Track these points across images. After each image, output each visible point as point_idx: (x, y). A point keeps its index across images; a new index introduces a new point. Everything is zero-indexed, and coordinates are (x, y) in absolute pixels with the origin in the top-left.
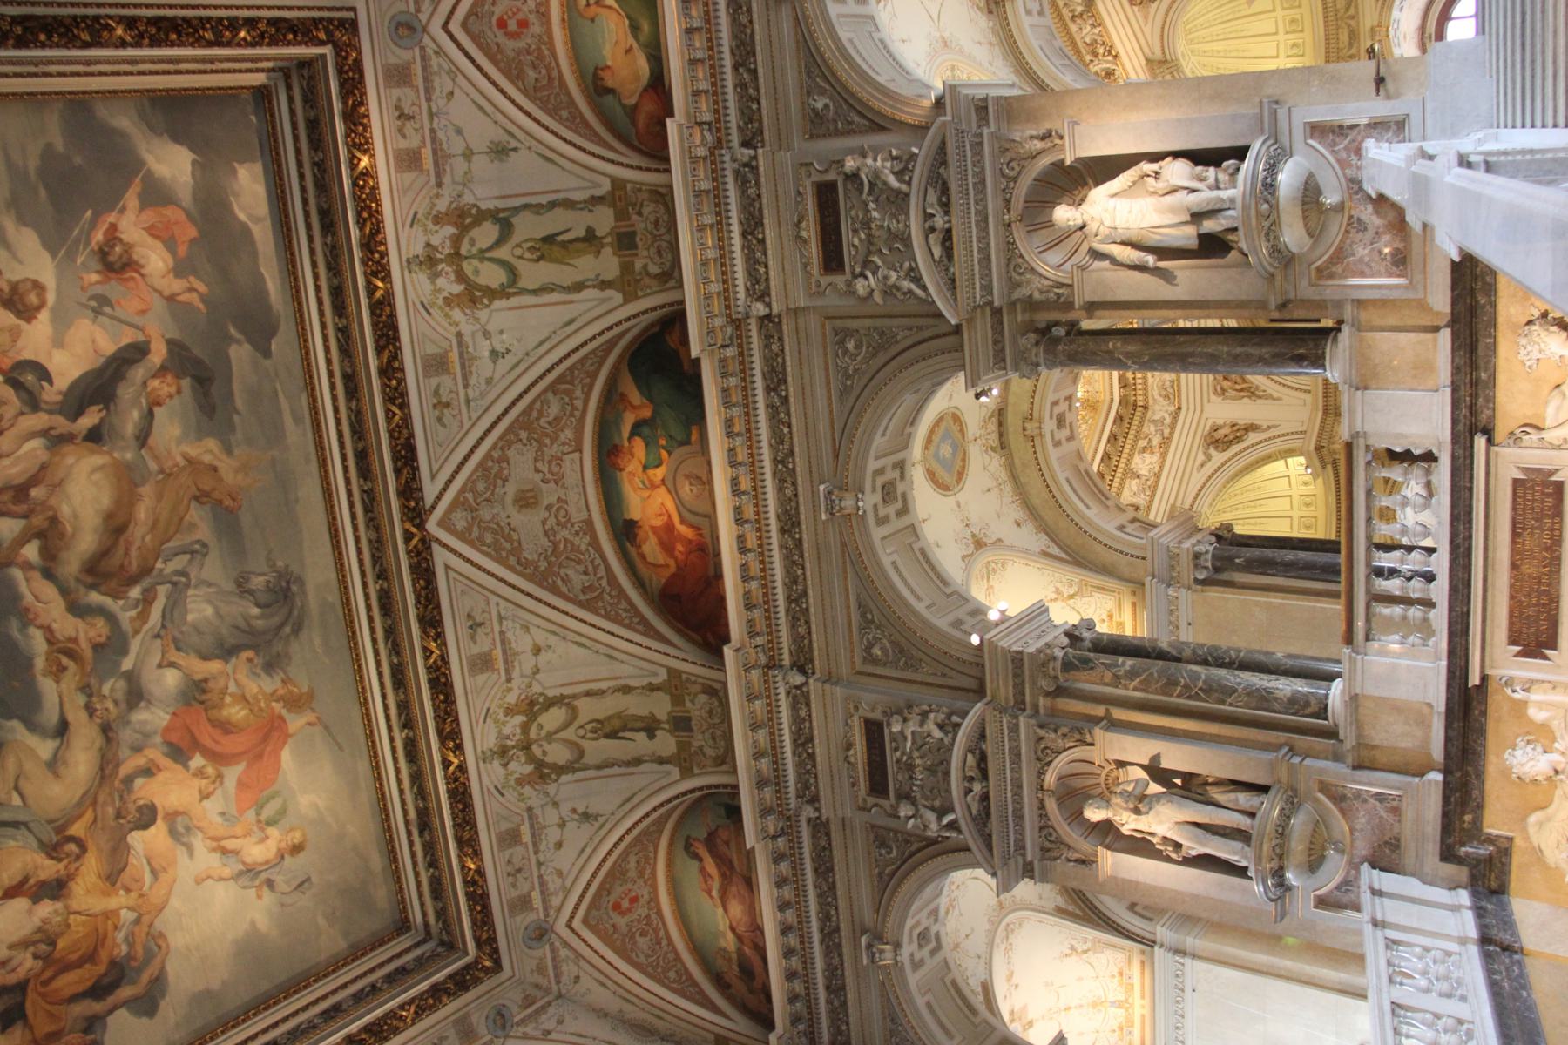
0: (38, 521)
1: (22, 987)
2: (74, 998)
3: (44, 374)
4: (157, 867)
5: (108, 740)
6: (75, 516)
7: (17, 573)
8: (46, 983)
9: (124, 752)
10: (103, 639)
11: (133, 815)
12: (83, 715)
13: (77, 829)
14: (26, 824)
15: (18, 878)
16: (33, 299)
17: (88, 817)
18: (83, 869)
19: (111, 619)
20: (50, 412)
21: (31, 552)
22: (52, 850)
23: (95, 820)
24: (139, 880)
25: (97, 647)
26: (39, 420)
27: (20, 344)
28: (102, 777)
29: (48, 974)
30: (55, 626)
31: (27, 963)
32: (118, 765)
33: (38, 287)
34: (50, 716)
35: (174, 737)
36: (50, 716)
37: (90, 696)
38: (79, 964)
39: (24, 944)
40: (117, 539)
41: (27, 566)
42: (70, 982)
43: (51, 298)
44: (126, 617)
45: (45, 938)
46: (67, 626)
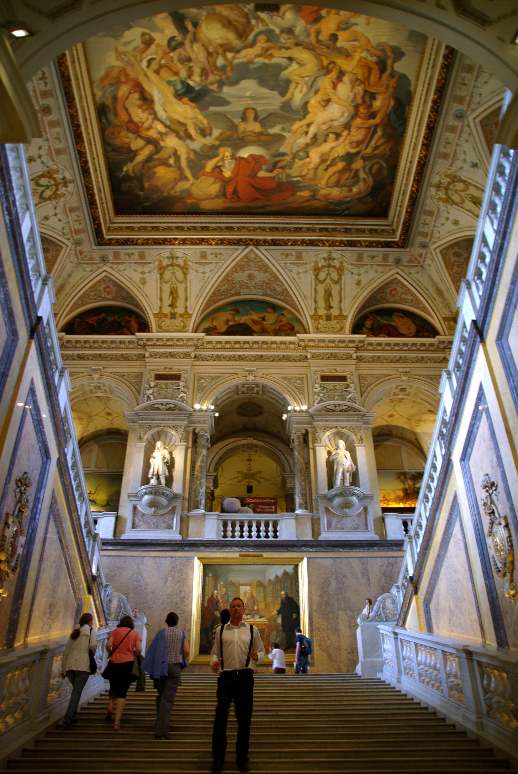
0: (220, 51)
1: (366, 92)
2: (380, 78)
3: (172, 39)
4: (353, 39)
5: (301, 45)
6: (221, 38)
7: (236, 61)
8: (369, 85)
9: (307, 40)
10: (266, 38)
11: (330, 43)
12: (289, 51)
13: (325, 62)
14: (316, 78)
15: (332, 84)
16: (147, 37)
17: (323, 58)
18: (340, 64)
19: (260, 33)
20: (185, 39)
21: (230, 55)
22: (328, 72)
23: (326, 56)
24: (355, 47)
25: (268, 41)
26: (187, 43)
27: (162, 44)
28: (312, 50)
29: (367, 84)
30: (256, 53)
31: (360, 89)
32: (311, 44)
33: (143, 34)
34: (284, 62)
35: (311, 19)
36: (284, 62)
37: (283, 47)
38: (370, 72)
39: (353, 88)
40: (233, 25)
41: (234, 58)
42: (373, 79)
43: (147, 31)
44: (261, 27)
45: (355, 82)
46: (257, 49)
